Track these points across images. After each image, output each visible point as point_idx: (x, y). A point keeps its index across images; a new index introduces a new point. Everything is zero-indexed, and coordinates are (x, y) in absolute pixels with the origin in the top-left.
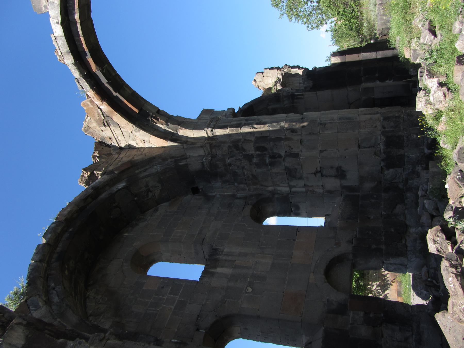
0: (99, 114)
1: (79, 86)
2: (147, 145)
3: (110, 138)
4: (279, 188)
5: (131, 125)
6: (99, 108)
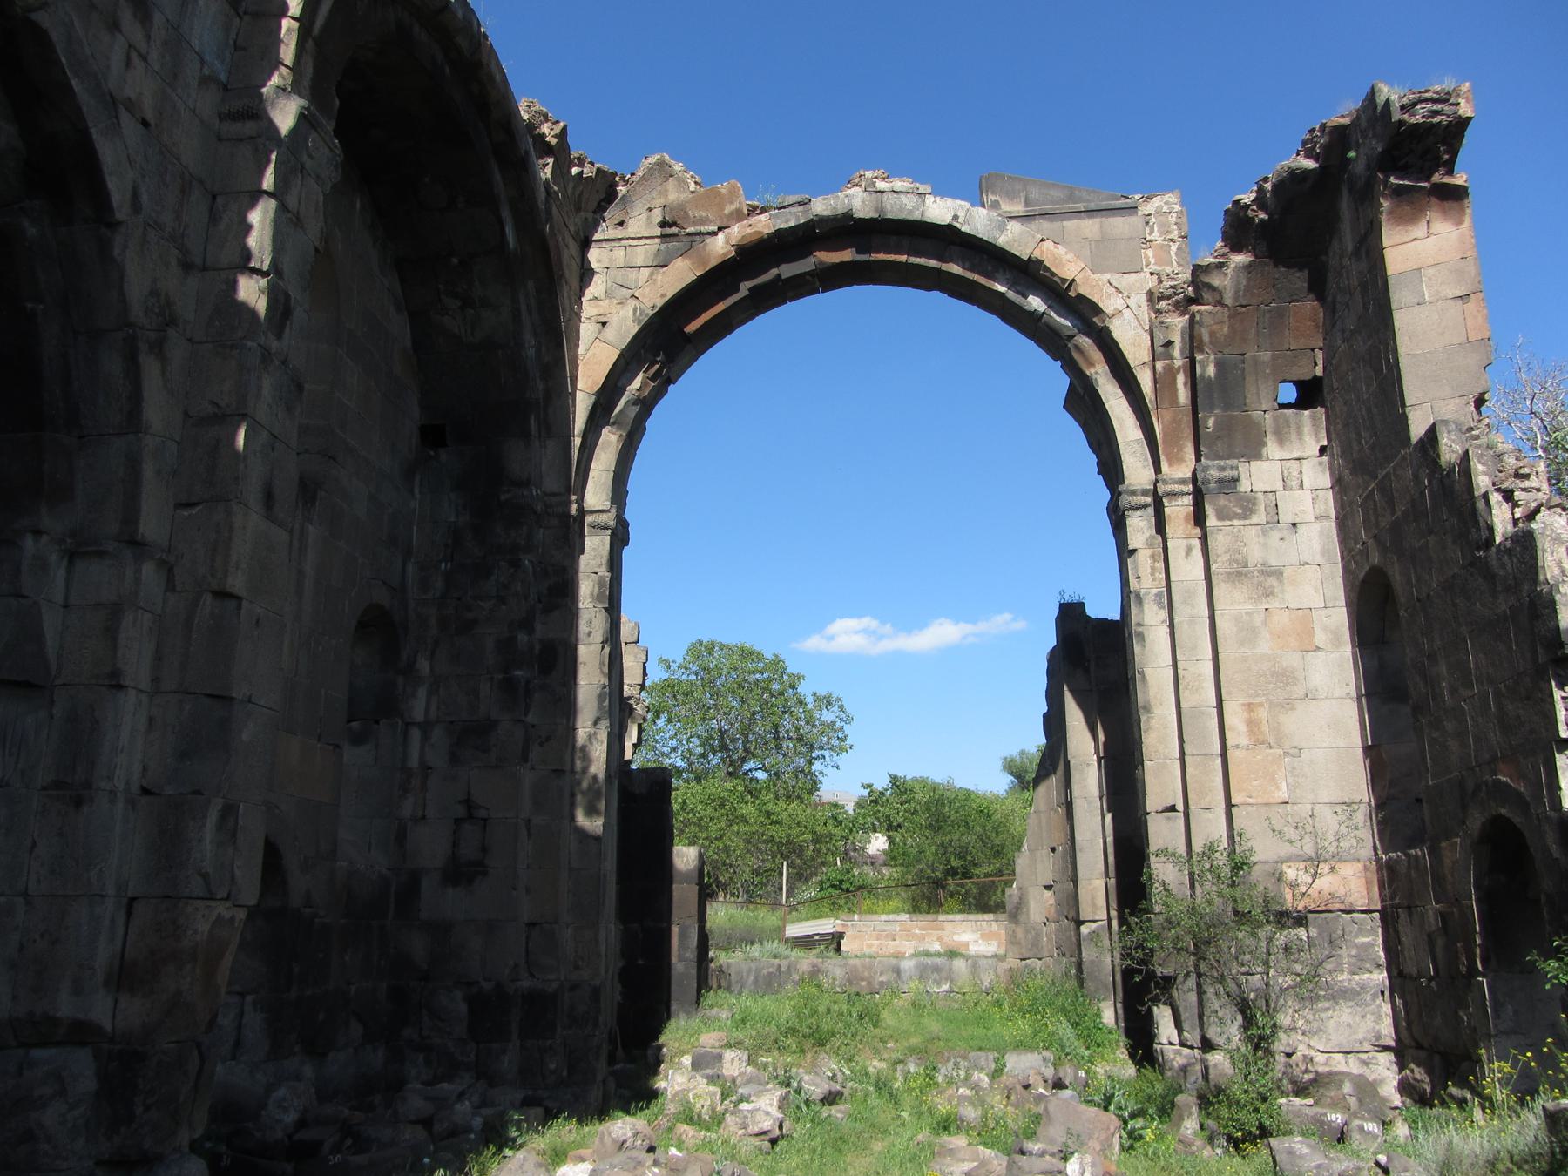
0: (702, 221)
1: (789, 199)
2: (587, 330)
3: (621, 224)
4: (422, 693)
5: (660, 303)
6: (720, 229)
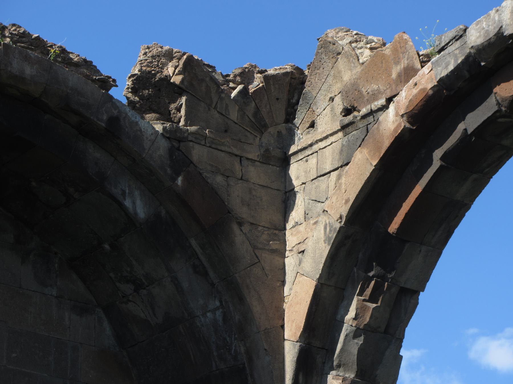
1: (445, 39)
3: (312, 125)
5: (344, 210)
6: (389, 100)
